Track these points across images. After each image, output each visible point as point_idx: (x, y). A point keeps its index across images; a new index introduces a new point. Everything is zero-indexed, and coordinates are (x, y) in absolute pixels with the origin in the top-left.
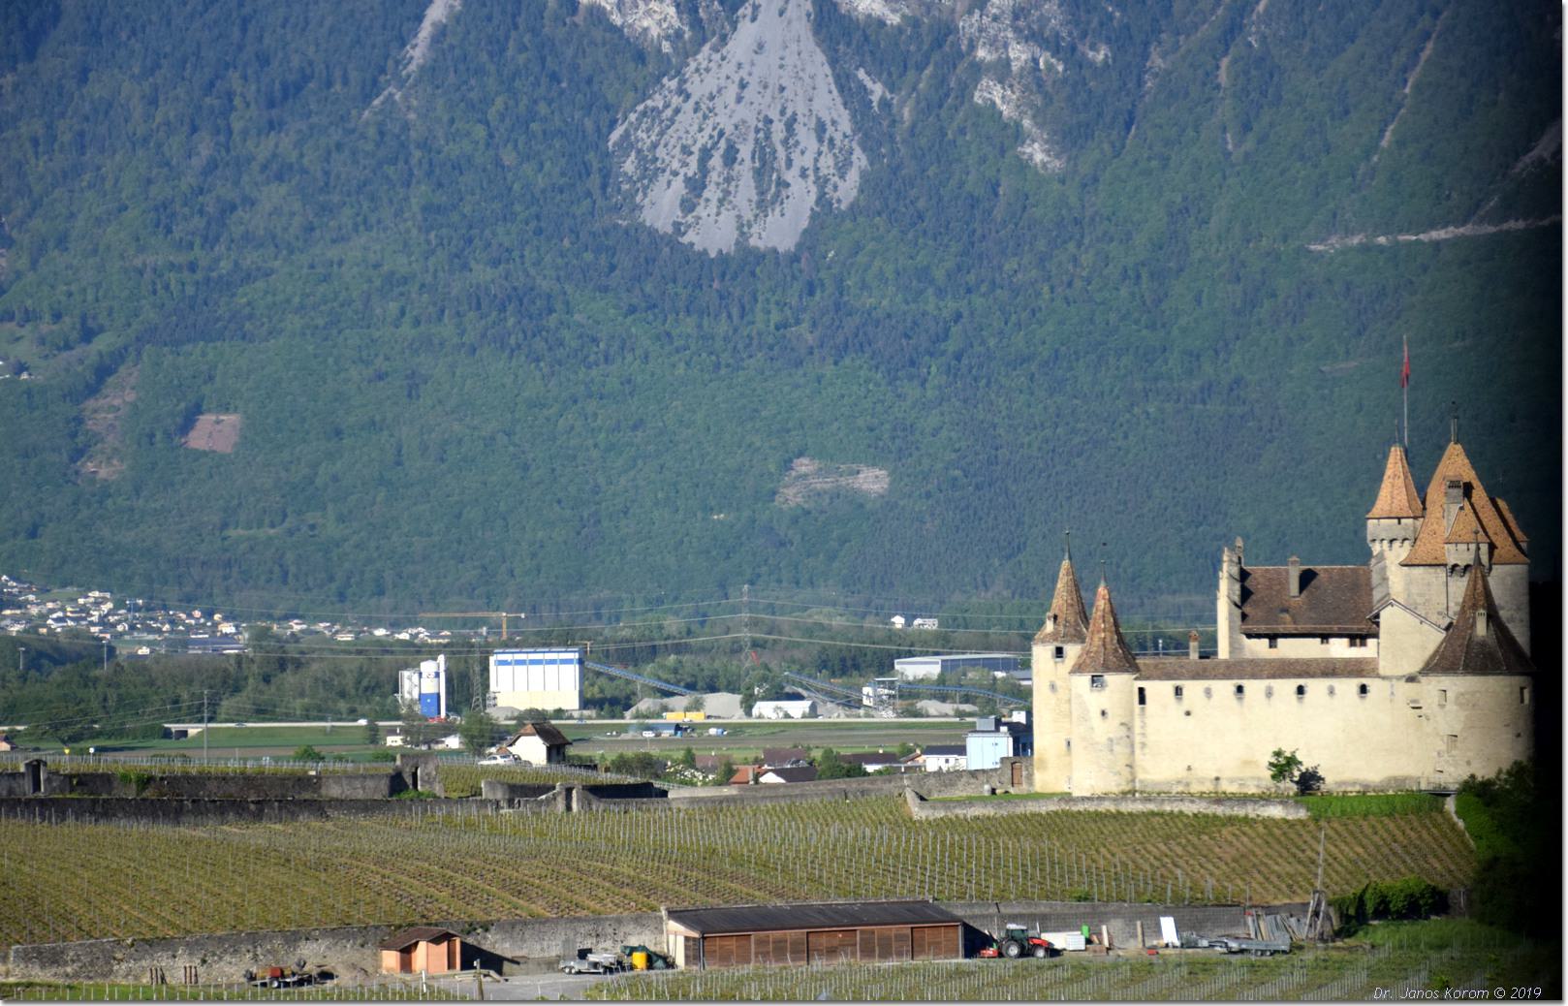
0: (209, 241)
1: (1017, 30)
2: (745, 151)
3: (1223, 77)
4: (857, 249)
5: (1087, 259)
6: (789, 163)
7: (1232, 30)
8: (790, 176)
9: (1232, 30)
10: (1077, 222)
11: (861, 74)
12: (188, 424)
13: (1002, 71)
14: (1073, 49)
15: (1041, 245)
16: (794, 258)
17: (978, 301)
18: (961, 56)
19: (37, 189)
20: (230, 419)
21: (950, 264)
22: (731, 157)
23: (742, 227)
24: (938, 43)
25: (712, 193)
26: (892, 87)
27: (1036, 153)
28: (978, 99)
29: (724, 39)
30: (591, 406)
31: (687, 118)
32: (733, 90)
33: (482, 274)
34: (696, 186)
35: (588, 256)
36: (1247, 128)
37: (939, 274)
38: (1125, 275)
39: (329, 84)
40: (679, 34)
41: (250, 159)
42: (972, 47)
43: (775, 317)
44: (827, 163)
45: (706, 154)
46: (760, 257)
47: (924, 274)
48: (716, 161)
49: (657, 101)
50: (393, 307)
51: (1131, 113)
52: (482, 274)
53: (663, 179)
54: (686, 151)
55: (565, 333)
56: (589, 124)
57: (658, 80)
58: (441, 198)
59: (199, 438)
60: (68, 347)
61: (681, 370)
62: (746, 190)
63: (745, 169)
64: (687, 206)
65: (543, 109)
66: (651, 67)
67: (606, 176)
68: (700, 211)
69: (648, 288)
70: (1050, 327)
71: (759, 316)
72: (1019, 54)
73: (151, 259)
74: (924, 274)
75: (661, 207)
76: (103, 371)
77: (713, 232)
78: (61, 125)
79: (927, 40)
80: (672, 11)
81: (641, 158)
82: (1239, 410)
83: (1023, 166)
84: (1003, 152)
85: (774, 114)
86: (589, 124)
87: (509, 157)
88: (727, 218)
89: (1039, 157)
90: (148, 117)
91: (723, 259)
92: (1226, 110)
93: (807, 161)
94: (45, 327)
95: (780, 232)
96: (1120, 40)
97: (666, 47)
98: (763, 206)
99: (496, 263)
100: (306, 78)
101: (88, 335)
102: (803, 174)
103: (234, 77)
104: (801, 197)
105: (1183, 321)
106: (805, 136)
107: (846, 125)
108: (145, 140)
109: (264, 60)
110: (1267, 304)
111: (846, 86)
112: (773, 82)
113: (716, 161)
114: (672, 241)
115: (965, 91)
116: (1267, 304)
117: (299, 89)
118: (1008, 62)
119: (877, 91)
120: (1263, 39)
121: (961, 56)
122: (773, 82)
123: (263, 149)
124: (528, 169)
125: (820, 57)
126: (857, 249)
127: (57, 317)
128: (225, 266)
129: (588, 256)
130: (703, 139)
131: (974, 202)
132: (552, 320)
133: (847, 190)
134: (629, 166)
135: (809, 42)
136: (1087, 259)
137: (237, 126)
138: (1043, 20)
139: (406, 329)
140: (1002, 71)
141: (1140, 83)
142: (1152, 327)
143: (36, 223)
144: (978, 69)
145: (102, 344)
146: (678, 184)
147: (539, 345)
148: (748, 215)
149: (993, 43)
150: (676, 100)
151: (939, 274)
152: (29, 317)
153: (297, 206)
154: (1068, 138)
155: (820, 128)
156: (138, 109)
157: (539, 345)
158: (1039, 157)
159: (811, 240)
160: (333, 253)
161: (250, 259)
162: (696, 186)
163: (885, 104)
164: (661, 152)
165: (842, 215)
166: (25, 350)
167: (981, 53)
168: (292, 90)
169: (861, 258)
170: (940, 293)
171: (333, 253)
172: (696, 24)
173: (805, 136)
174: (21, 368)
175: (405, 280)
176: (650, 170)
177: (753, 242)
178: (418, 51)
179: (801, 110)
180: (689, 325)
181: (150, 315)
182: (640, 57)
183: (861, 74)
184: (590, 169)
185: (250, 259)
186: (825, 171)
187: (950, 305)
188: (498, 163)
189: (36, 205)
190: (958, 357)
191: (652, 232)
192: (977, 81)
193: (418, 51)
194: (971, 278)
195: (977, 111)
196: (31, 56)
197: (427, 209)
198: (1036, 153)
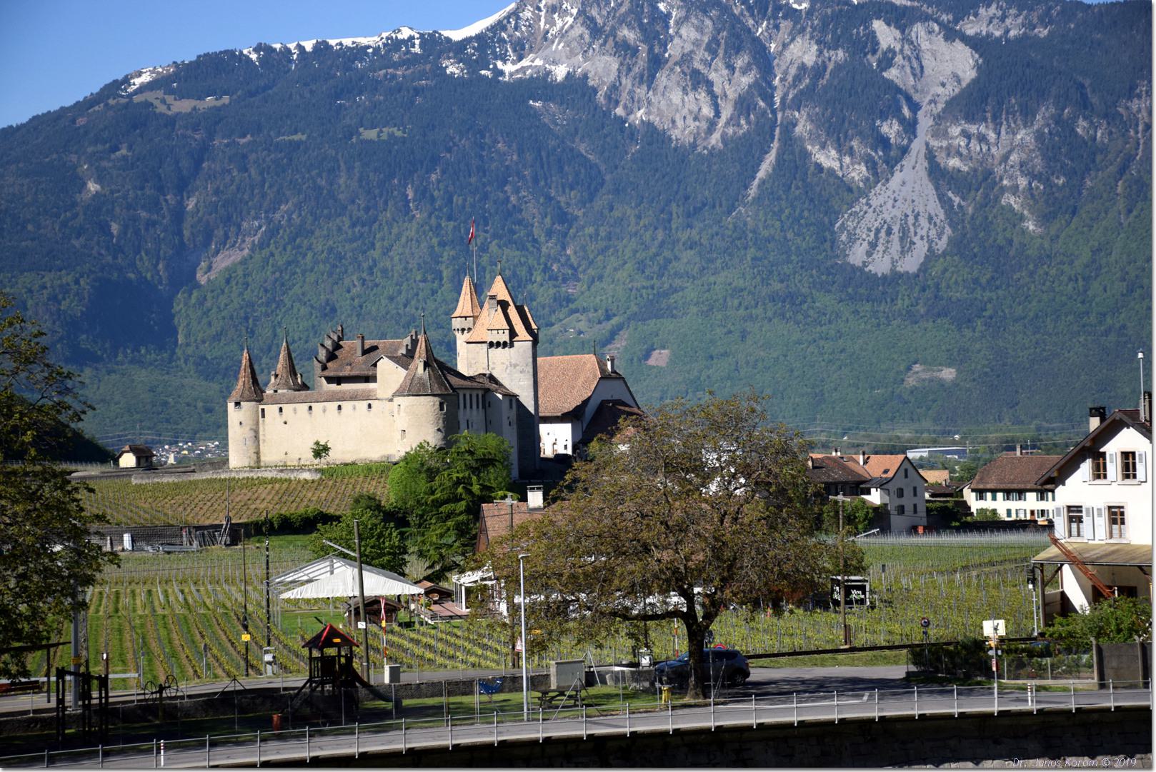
0: (660, 275)
1: (1022, 172)
2: (896, 229)
3: (1119, 190)
4: (945, 270)
5: (1053, 272)
6: (916, 234)
7: (1123, 169)
8: (916, 239)
9: (1123, 169)
10: (1048, 256)
11: (950, 194)
12: (647, 356)
13: (1014, 190)
14: (1048, 179)
15: (1031, 267)
16: (918, 276)
17: (1000, 292)
18: (995, 183)
19: (591, 257)
20: (665, 352)
21: (988, 276)
22: (889, 232)
23: (893, 262)
24: (985, 179)
25: (880, 248)
26: (963, 199)
27: (1031, 226)
28: (1003, 202)
29: (887, 180)
30: (822, 343)
31: (870, 215)
32: (891, 202)
33: (777, 286)
34: (873, 245)
35: (824, 277)
36: (1130, 211)
37: (983, 281)
38: (1070, 279)
39: (714, 207)
40: (867, 179)
41: (678, 241)
42: (1001, 179)
43: (907, 302)
44: (933, 233)
45: (878, 231)
46: (901, 275)
47: (976, 281)
48: (883, 234)
49: (857, 209)
50: (736, 302)
51: (1075, 208)
52: (777, 286)
53: (858, 242)
54: (869, 230)
55: (811, 312)
56: (826, 220)
57: (857, 200)
58: (759, 254)
59: (652, 362)
60: (600, 322)
61: (863, 326)
62: (896, 246)
63: (895, 237)
64: (869, 254)
65: (806, 214)
66: (856, 194)
67: (833, 242)
68: (875, 256)
69: (850, 290)
70: (1034, 303)
71: (900, 302)
72: (1023, 182)
73: (635, 284)
74: (976, 281)
75: (857, 255)
76: (613, 334)
77: (880, 265)
78: (602, 229)
79: (980, 178)
80: (864, 169)
81: (849, 233)
82: (1124, 339)
83: (1024, 232)
84: (1014, 226)
85: (909, 213)
86: (826, 220)
87: (790, 235)
88: (887, 259)
89: (1031, 227)
90: (637, 224)
91: (884, 277)
92: (1121, 204)
93: (924, 233)
94: (591, 315)
95: (910, 264)
96: (1071, 174)
97: (861, 185)
98: (903, 253)
99: (782, 281)
100: (704, 205)
101: (608, 318)
102: (922, 238)
103: (674, 205)
104: (921, 249)
105: (1097, 299)
106: (923, 222)
107: (942, 216)
108: (636, 234)
109: (687, 198)
110: (1139, 291)
111: (942, 198)
112: (909, 199)
113: (883, 234)
114: (861, 270)
115: (997, 199)
116: (1139, 291)
117: (701, 209)
118: (1017, 186)
119: (957, 200)
120: (1139, 172)
121: (995, 183)
122: (909, 199)
123: (684, 236)
124: (799, 241)
125: (931, 186)
126: (945, 270)
127: (596, 311)
128: (666, 286)
129: (824, 277)
130: (877, 224)
131: (1001, 248)
132: (805, 307)
133: (942, 245)
134: (844, 237)
135: (926, 180)
136: (1053, 272)
137: (674, 226)
138: (1034, 167)
139: (742, 311)
140: (1014, 190)
141: (1080, 193)
142: (1083, 302)
143: (591, 271)
144: (1003, 190)
145: (614, 321)
146: (865, 244)
147: (800, 317)
148: (896, 257)
149: (1011, 177)
150: (865, 208)
151: (983, 281)
152: (585, 310)
153: (697, 259)
154: (1045, 219)
155: (930, 219)
156: (633, 220)
157: (800, 317)
158: (1031, 227)
159: (924, 268)
160: (712, 279)
161: (677, 282)
162: (873, 245)
163: (960, 206)
164: (858, 231)
165: (939, 256)
166: (582, 325)
167: (1005, 182)
168: (698, 210)
169: (948, 275)
170: (984, 289)
171: (712, 279)
172: (876, 174)
173: (923, 222)
174: (580, 332)
175: (742, 290)
176: (853, 238)
177: (899, 269)
178: (753, 191)
179: (921, 209)
180: (868, 307)
181: (634, 308)
182: (850, 190)
183: (950, 194)
184: (826, 237)
185: (677, 282)
186: (932, 236)
187: (987, 294)
188: (785, 238)
189: (591, 263)
190: (991, 318)
191: (853, 266)
192: (1003, 194)
193: (753, 191)
194: (998, 283)
195: (1003, 208)
196: (591, 201)
197: (754, 259)
198: (1031, 226)
